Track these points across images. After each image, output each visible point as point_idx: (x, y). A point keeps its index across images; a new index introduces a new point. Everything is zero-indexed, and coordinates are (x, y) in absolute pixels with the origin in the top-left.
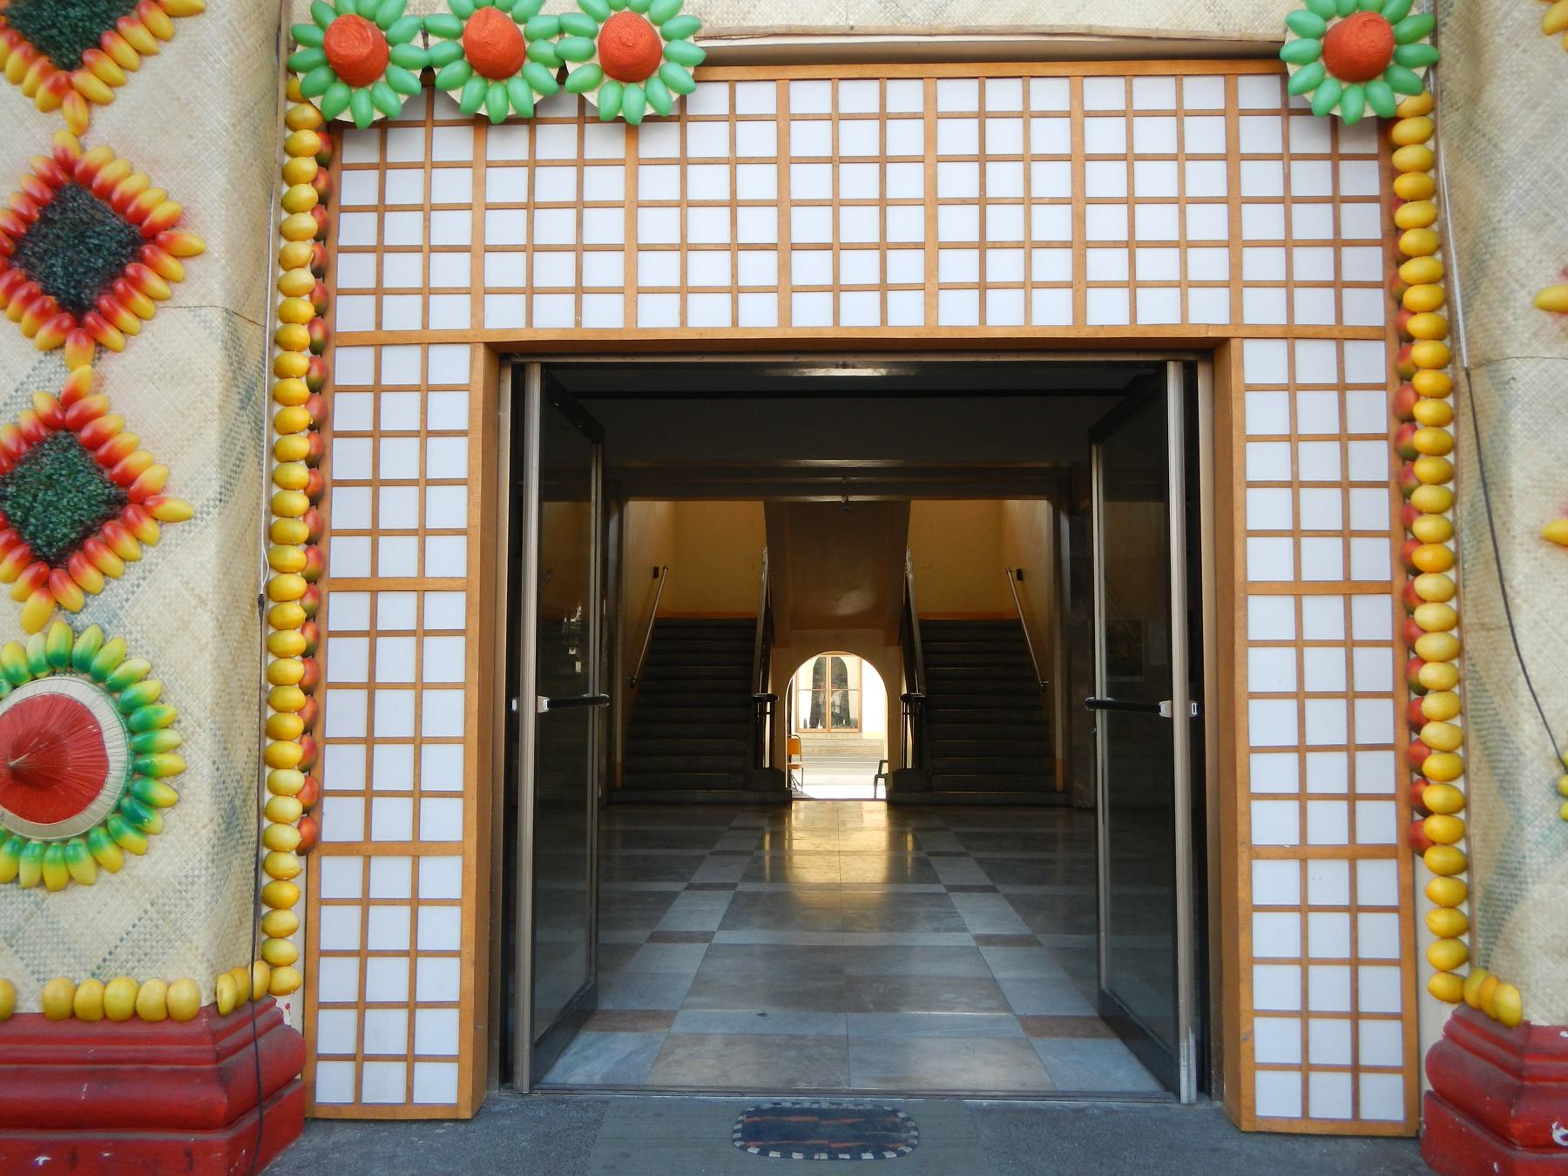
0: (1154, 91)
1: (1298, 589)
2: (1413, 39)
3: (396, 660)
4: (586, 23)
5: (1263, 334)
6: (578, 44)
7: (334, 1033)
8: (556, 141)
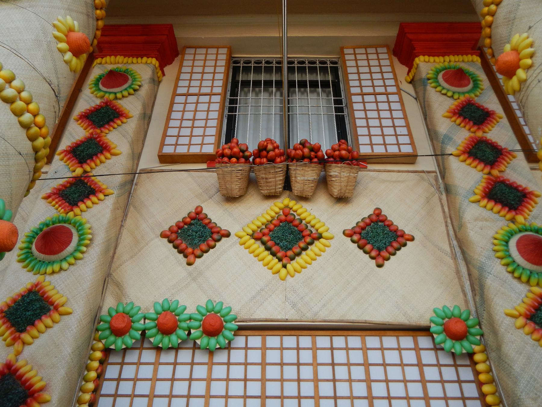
0: (390, 341)
2: (473, 327)
4: (199, 317)
6: (196, 324)
8: (185, 356)
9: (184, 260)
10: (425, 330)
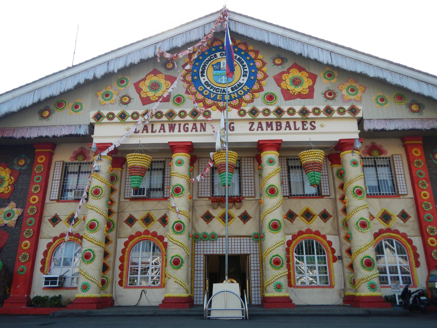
1: (254, 270)
3: (199, 275)
5: (252, 254)
7: (195, 299)
8: (208, 241)
9: (206, 223)
10: (251, 236)
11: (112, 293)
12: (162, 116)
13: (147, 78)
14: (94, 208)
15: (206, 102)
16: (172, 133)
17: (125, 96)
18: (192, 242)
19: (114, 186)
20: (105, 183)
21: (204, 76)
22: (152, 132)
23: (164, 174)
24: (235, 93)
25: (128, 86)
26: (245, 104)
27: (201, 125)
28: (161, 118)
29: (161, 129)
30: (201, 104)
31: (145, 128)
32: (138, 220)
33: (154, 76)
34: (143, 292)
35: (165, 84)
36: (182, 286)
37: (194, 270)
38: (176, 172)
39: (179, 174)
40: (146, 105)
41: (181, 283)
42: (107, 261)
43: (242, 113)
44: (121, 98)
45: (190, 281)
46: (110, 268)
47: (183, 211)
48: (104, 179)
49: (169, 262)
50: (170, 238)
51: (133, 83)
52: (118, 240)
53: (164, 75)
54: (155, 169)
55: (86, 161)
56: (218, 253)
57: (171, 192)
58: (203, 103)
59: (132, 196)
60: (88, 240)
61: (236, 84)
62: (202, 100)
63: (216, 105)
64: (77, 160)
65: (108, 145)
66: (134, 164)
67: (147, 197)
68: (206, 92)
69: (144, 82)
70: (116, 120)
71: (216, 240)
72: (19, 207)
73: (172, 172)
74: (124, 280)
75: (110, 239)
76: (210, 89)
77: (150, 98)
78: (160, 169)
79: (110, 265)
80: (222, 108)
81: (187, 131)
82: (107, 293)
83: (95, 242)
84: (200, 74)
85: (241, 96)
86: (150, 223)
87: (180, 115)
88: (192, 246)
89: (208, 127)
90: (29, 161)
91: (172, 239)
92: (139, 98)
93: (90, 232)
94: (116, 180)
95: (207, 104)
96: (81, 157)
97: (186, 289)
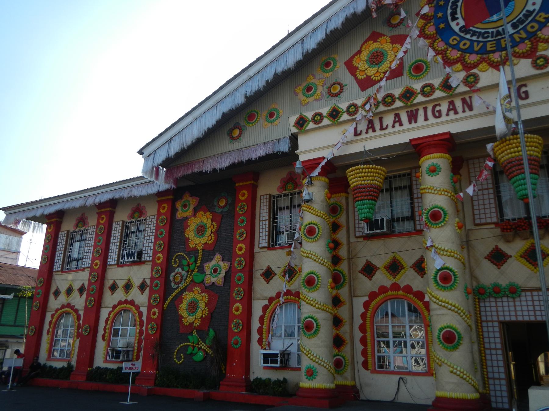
6: (507, 290)
9: (496, 267)
11: (355, 380)
12: (393, 101)
13: (363, 49)
14: (310, 256)
15: (466, 60)
16: (413, 125)
17: (334, 84)
18: (475, 301)
19: (339, 220)
20: (322, 217)
21: (458, 18)
22: (382, 129)
23: (411, 194)
24: (522, 32)
25: (336, 69)
26: (545, 45)
27: (464, 101)
28: (393, 104)
29: (395, 122)
30: (459, 66)
31: (371, 126)
32: (379, 268)
33: (373, 43)
34: (401, 380)
35: (392, 50)
36: (465, 379)
37: (484, 347)
38: (429, 187)
39: (435, 188)
40: (367, 90)
41: (462, 374)
42: (341, 331)
43: (541, 63)
44: (329, 89)
45: (479, 367)
46: (347, 342)
47: (450, 250)
48: (319, 211)
49: (437, 337)
50: (433, 296)
51: (343, 62)
52: (355, 299)
53: (389, 37)
54: (396, 189)
55: (297, 190)
56: (526, 319)
57: (424, 220)
58: (462, 64)
59: (366, 232)
60: (307, 303)
61: (521, 16)
62: (458, 59)
63: (486, 62)
64: (286, 190)
65: (319, 161)
66: (357, 183)
67: (388, 232)
68: (465, 44)
69: (358, 56)
70: (326, 122)
71: (520, 296)
72: (226, 260)
73: (422, 187)
74: (370, 360)
75: (342, 299)
76: (471, 36)
77: (372, 77)
78: (405, 187)
79: (347, 337)
80: (498, 64)
81: (440, 116)
82: (346, 379)
83: (317, 306)
84: (449, 18)
85: (535, 33)
86: (399, 272)
87: (423, 92)
88: (475, 307)
89: (477, 101)
90: (230, 199)
91: (436, 298)
92: (355, 81)
93: (308, 290)
94: (341, 211)
95: (470, 63)
96: (290, 186)
97: (473, 385)
